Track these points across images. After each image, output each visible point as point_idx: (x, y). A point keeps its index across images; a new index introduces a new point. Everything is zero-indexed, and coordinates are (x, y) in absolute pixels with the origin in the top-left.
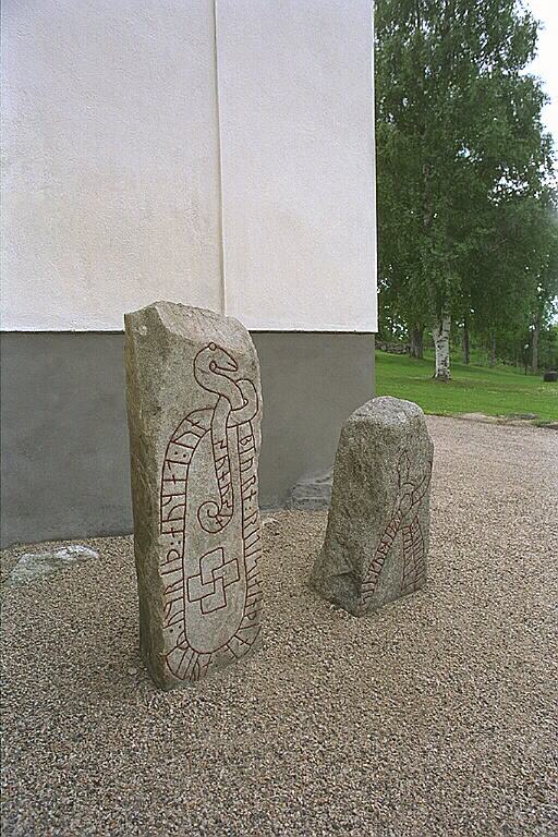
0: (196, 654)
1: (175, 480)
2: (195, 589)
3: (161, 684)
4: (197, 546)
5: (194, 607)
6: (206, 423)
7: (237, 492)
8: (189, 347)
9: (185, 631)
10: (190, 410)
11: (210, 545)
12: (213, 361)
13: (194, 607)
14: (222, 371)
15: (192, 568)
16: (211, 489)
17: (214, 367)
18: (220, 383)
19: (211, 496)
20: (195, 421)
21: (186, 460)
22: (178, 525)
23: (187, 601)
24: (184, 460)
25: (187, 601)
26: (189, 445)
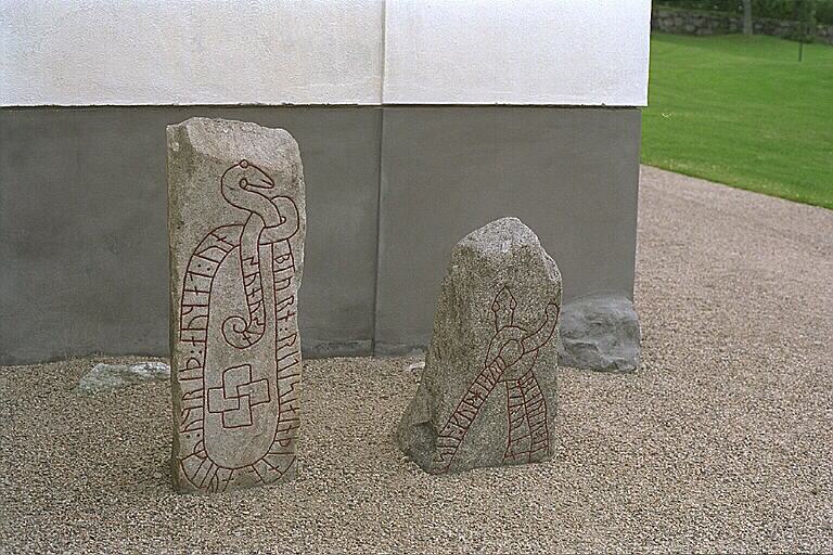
0: (215, 468)
1: (197, 292)
2: (214, 399)
3: (177, 488)
4: (221, 358)
5: (213, 419)
6: (235, 239)
7: (271, 311)
8: (216, 165)
9: (203, 440)
10: (216, 225)
11: (236, 358)
13: (213, 419)
14: (254, 188)
15: (213, 379)
16: (240, 303)
17: (244, 184)
18: (251, 199)
19: (237, 310)
20: (221, 236)
21: (211, 273)
22: (200, 335)
23: (207, 412)
24: (208, 273)
25: (207, 412)
26: (214, 259)
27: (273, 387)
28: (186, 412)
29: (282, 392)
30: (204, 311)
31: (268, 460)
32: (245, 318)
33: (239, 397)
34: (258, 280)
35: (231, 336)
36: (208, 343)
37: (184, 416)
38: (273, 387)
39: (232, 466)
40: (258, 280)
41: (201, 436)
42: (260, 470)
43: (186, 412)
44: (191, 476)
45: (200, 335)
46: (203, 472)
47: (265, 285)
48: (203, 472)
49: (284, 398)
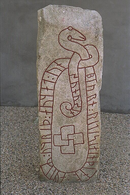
12: (70, 36)
14: (75, 41)
23: (53, 145)
25: (53, 145)
27: (85, 137)
28: (43, 144)
29: (90, 140)
30: (51, 98)
31: (83, 170)
32: (71, 103)
33: (69, 140)
34: (78, 86)
35: (65, 111)
36: (53, 114)
37: (42, 146)
38: (85, 137)
39: (65, 171)
40: (78, 86)
41: (50, 156)
42: (79, 174)
43: (43, 144)
44: (46, 173)
45: (49, 110)
46: (51, 172)
47: (81, 88)
48: (51, 172)
49: (91, 143)
